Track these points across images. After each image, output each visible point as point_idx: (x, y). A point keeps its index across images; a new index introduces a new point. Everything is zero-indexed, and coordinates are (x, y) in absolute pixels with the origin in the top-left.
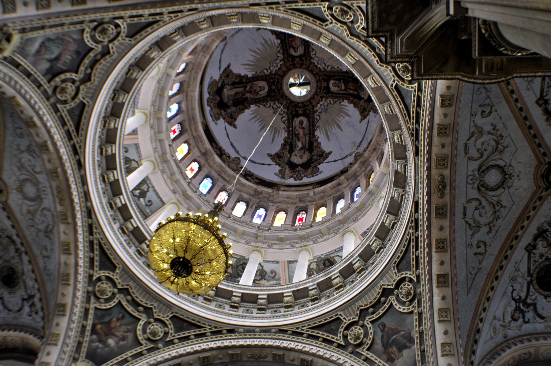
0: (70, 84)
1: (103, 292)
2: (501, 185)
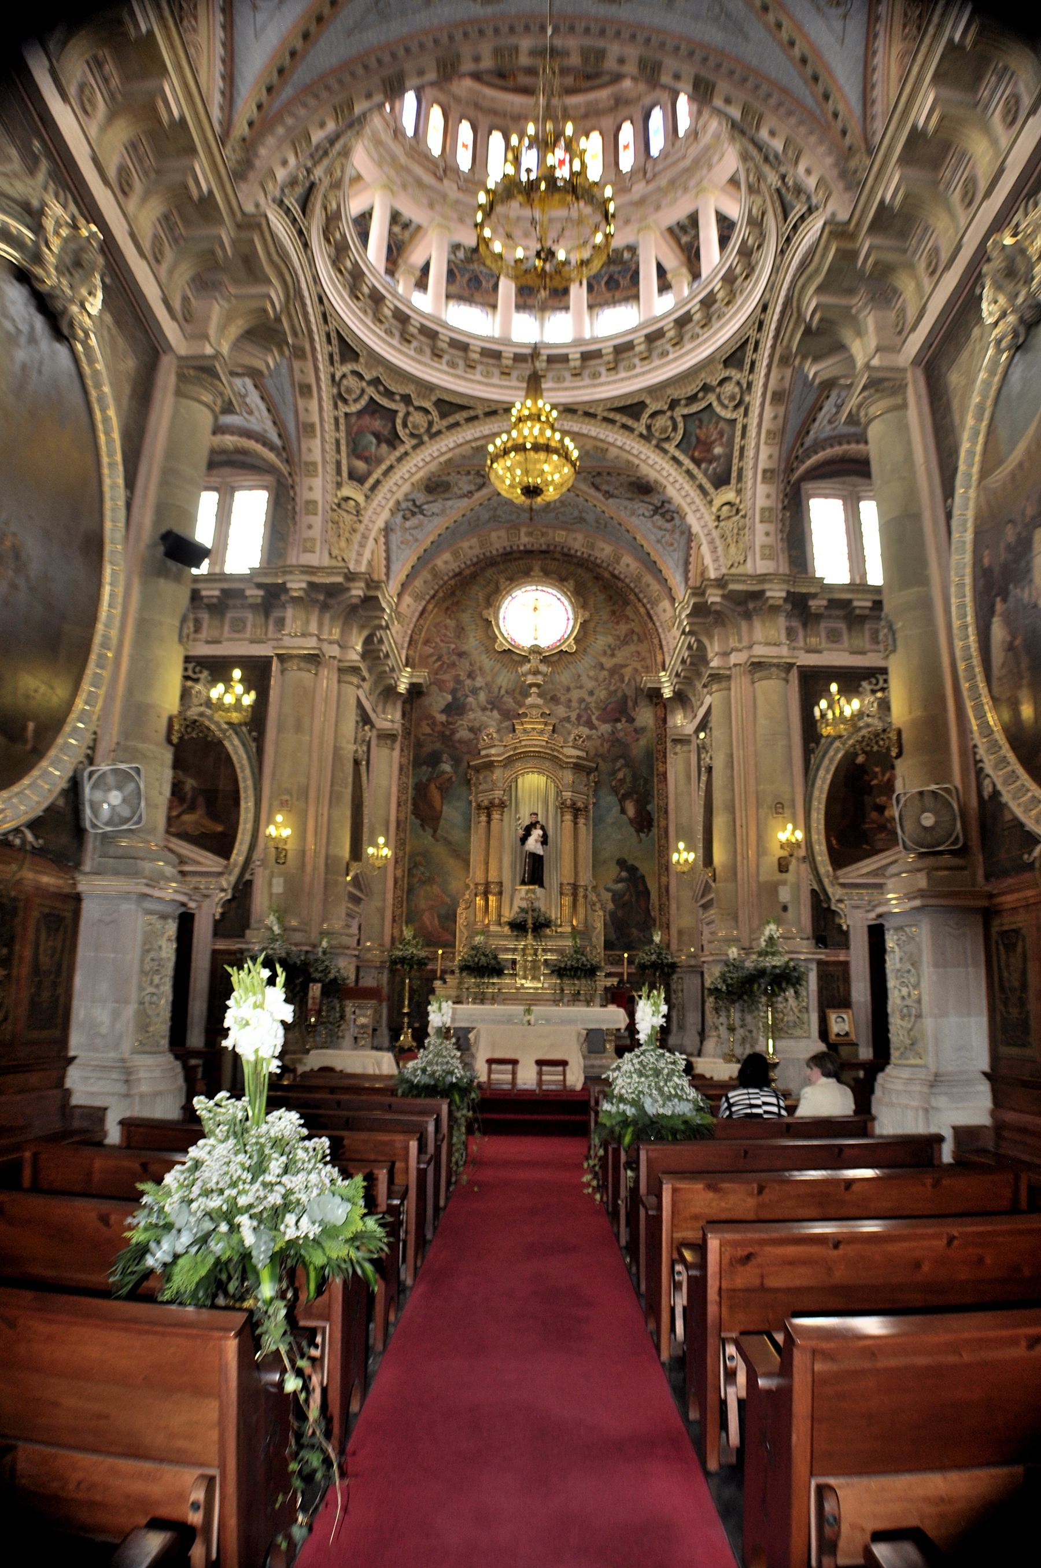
0: (411, 419)
1: (664, 430)
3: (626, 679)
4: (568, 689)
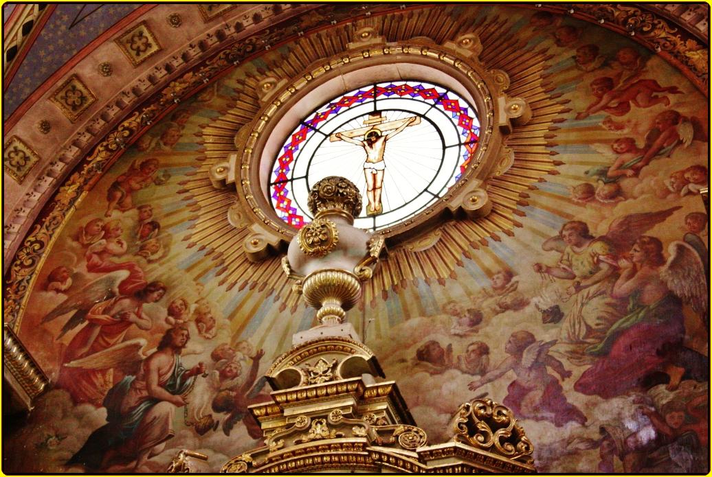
3: (671, 252)
4: (477, 320)
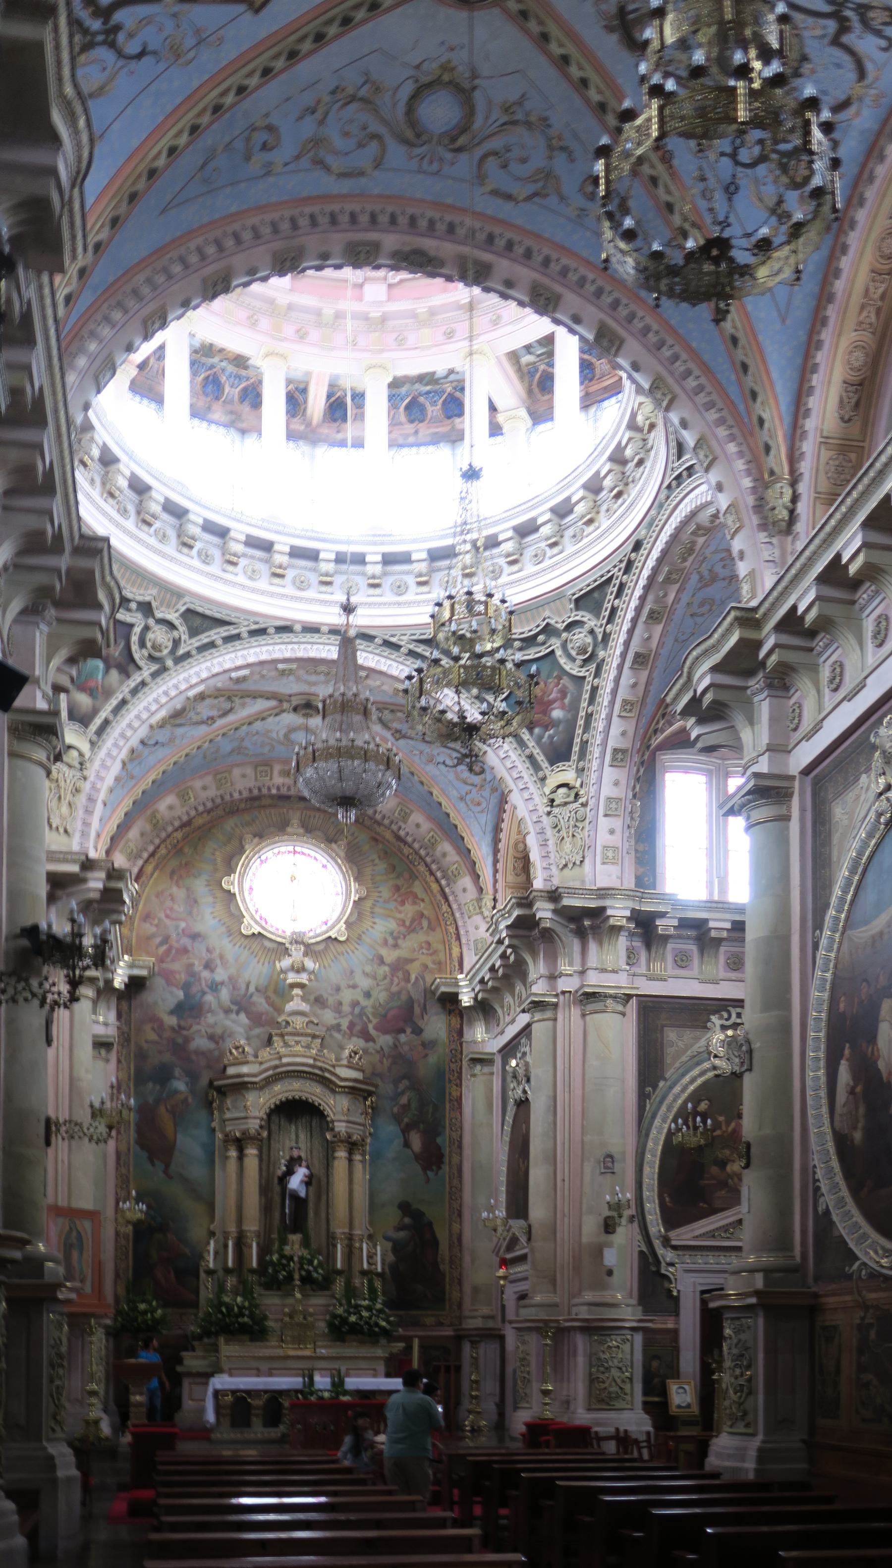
2: (464, 94)
